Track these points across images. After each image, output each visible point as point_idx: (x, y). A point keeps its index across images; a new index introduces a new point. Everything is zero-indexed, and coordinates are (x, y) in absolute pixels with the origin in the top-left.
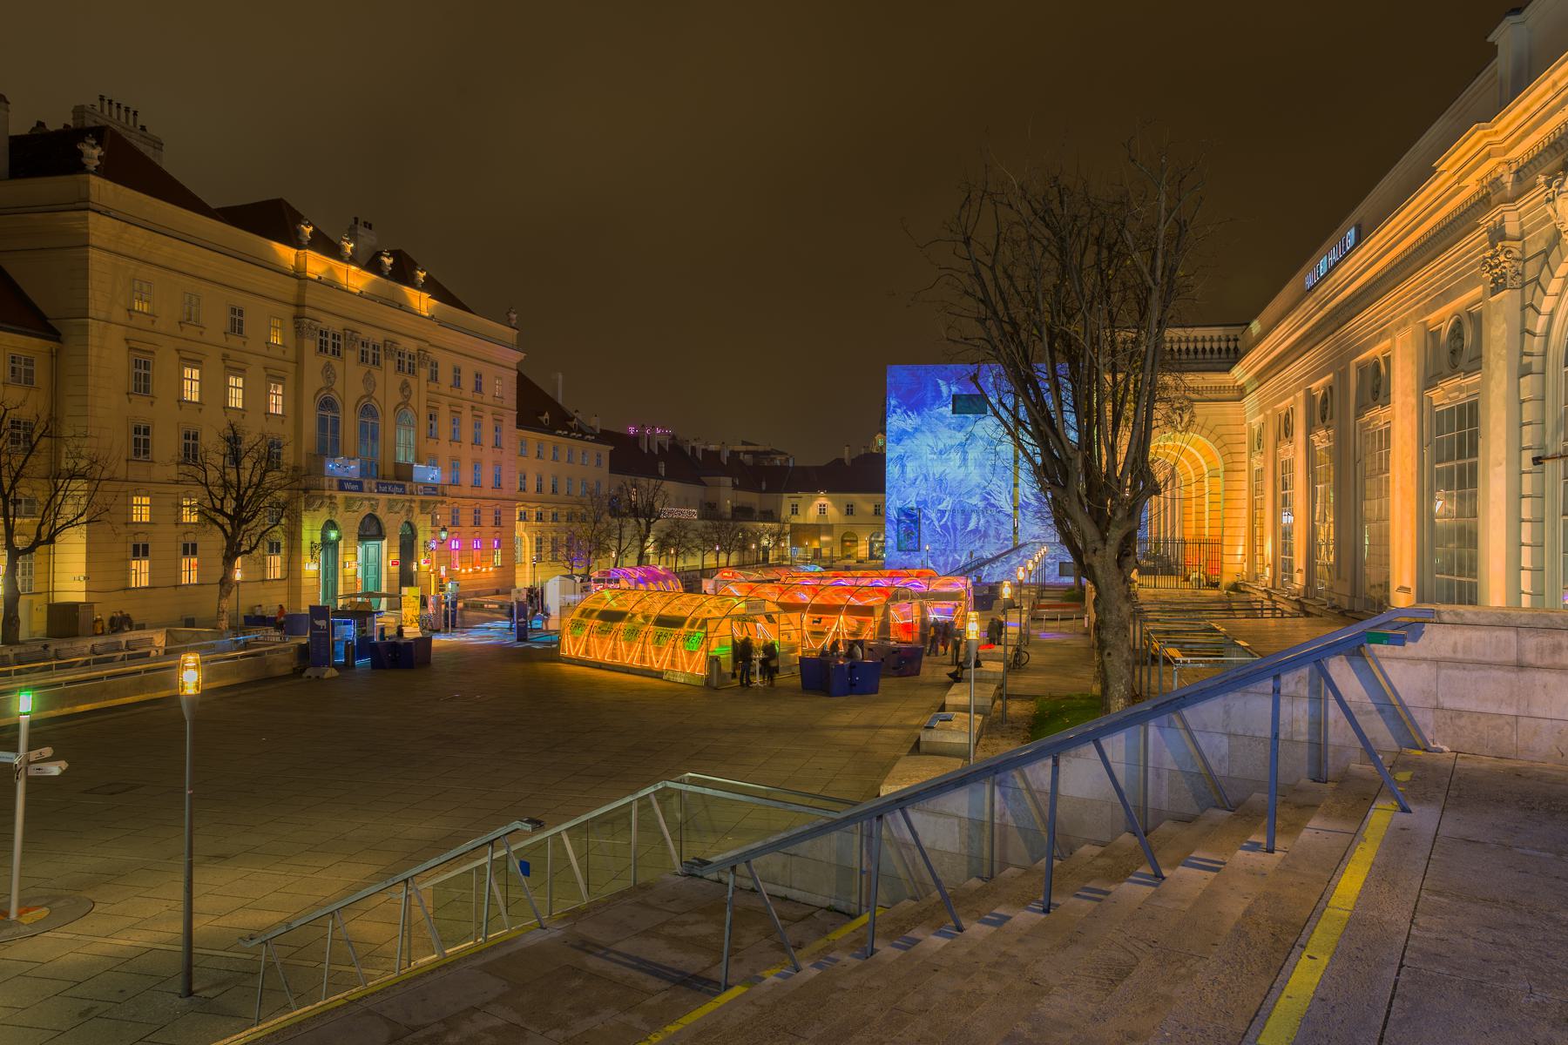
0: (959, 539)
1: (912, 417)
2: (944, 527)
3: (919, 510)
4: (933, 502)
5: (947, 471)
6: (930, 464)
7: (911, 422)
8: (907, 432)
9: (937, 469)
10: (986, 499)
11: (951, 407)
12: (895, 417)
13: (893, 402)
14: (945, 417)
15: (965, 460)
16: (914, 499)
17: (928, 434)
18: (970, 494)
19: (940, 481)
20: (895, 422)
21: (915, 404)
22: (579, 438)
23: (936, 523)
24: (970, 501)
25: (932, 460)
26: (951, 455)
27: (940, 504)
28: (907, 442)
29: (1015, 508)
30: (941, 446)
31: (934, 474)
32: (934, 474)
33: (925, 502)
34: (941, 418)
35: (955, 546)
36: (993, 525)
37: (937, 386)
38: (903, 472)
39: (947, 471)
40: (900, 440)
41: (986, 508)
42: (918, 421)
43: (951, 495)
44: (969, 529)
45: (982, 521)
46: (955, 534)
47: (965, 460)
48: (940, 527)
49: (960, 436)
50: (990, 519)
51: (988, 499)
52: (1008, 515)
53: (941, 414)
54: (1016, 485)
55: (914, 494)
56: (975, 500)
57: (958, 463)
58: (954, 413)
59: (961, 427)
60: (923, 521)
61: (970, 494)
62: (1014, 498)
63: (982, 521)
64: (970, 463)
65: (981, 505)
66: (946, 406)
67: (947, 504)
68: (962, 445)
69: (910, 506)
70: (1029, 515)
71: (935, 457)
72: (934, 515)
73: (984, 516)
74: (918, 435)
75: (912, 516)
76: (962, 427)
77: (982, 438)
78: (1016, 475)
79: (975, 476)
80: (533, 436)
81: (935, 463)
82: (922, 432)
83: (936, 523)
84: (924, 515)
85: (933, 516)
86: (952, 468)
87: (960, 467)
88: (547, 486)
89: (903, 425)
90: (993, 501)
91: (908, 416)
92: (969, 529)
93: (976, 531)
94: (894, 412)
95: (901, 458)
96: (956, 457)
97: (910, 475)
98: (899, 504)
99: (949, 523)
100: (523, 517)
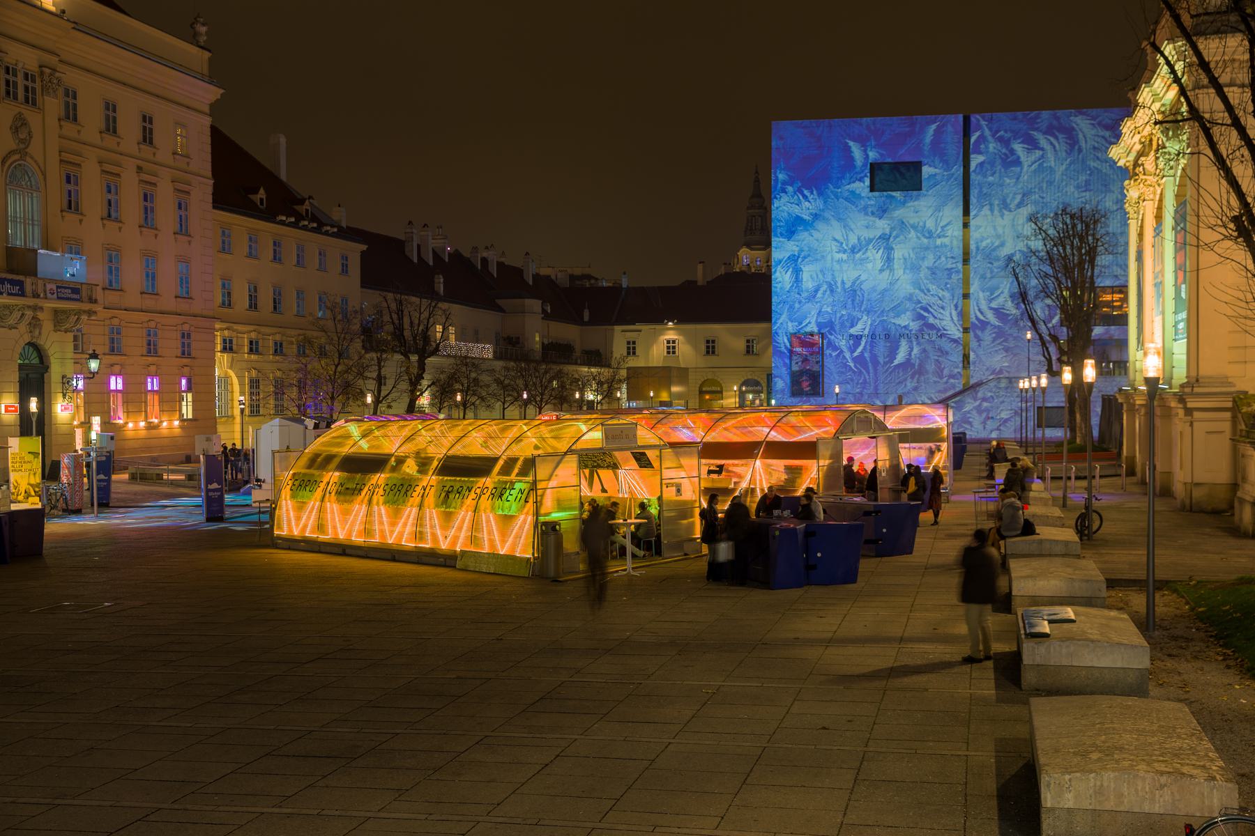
2: (859, 360)
3: (823, 336)
4: (842, 324)
5: (862, 278)
6: (837, 267)
9: (848, 275)
16: (813, 321)
17: (834, 223)
18: (897, 310)
19: (853, 293)
23: (847, 355)
25: (840, 261)
26: (869, 254)
27: (852, 326)
30: (853, 240)
31: (843, 282)
32: (843, 282)
33: (830, 324)
35: (876, 388)
38: (797, 280)
39: (862, 278)
43: (868, 312)
48: (855, 360)
49: (882, 225)
54: (966, 296)
55: (814, 312)
57: (879, 265)
60: (827, 352)
61: (897, 310)
62: (963, 315)
67: (862, 326)
68: (885, 238)
69: (808, 329)
71: (845, 257)
72: (843, 343)
75: (812, 345)
81: (845, 267)
83: (847, 355)
84: (830, 344)
85: (843, 344)
87: (881, 271)
96: (876, 257)
97: (808, 283)
98: (791, 327)
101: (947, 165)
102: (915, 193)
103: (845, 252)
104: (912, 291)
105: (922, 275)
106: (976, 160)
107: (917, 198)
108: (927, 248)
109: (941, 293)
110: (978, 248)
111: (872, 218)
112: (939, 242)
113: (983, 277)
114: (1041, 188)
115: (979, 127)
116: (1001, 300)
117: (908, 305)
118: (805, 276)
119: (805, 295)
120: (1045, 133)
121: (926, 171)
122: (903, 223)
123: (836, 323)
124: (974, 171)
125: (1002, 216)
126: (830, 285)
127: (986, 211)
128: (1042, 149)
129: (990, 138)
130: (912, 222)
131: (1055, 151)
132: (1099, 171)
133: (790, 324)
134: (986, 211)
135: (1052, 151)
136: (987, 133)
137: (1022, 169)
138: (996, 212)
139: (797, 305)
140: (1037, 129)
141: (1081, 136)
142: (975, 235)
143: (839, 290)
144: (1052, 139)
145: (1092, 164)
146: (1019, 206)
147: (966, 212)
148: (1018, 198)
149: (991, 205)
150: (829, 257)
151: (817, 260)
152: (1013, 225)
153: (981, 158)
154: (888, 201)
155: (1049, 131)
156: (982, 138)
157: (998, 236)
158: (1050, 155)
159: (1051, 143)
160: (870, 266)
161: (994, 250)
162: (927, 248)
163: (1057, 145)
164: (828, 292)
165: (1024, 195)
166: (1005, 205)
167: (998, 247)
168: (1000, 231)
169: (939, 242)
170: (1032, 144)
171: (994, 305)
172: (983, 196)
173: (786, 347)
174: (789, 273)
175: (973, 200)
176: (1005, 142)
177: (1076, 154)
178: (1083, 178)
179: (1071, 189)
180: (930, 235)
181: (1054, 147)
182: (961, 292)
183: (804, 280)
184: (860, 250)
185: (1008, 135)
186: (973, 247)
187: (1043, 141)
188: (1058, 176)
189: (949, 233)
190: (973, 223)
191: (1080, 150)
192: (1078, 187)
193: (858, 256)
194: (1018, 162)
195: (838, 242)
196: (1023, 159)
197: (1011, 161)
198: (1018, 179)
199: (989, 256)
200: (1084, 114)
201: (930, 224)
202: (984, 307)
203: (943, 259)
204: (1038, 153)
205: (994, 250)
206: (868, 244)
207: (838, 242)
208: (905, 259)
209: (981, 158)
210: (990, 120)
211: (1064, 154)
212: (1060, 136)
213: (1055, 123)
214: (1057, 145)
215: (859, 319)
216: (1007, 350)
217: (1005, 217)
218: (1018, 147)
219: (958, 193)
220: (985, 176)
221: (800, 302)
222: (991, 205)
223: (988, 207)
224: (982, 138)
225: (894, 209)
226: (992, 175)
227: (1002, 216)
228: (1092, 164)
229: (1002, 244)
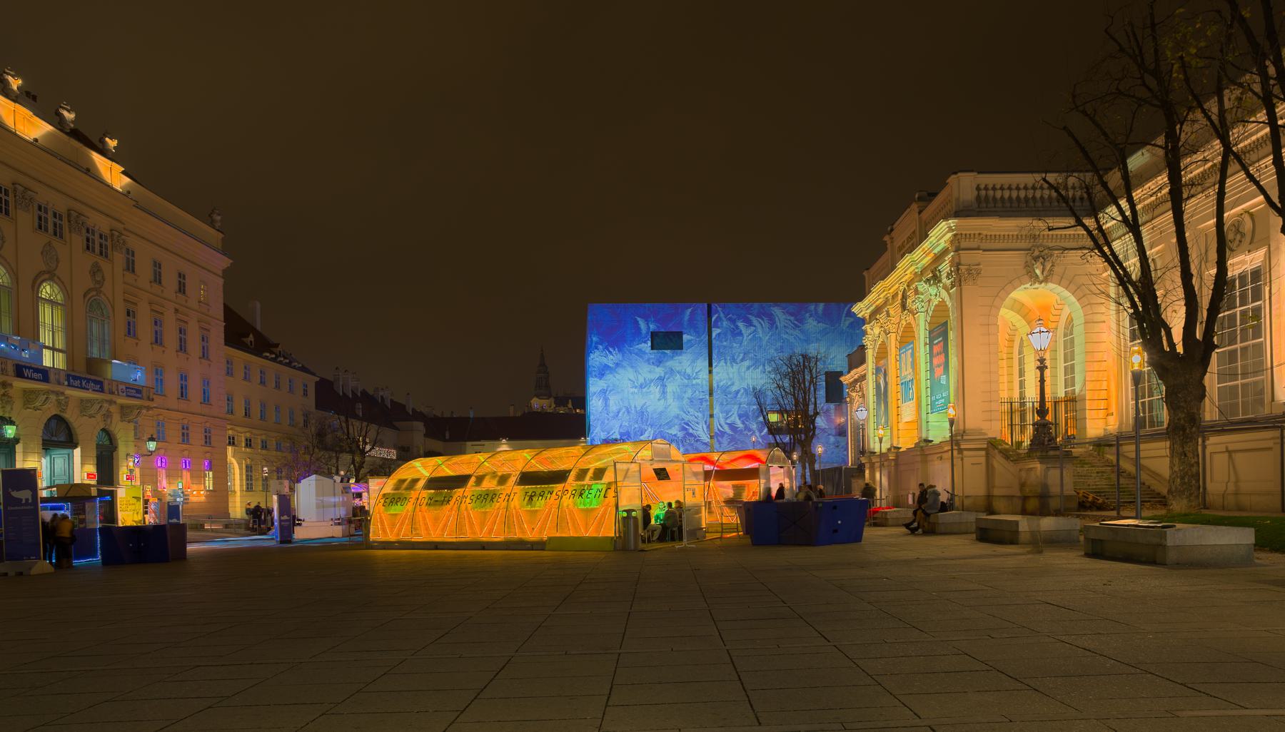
4: (635, 434)
5: (647, 404)
7: (611, 358)
8: (608, 366)
9: (638, 402)
11: (649, 344)
12: (597, 353)
13: (595, 339)
14: (645, 353)
15: (664, 393)
16: (617, 431)
17: (630, 370)
18: (670, 425)
19: (642, 413)
20: (596, 358)
21: (617, 339)
22: (286, 364)
24: (670, 431)
26: (651, 389)
27: (642, 435)
28: (610, 378)
29: (712, 437)
30: (641, 380)
31: (635, 407)
32: (635, 407)
34: (641, 353)
37: (636, 323)
38: (606, 405)
39: (647, 404)
40: (603, 375)
41: (684, 437)
42: (619, 356)
47: (664, 393)
49: (659, 371)
50: (689, 448)
51: (686, 429)
52: (705, 444)
53: (640, 350)
54: (711, 416)
55: (617, 426)
57: (658, 396)
58: (652, 349)
59: (659, 362)
61: (670, 425)
64: (669, 396)
65: (680, 434)
66: (645, 342)
68: (661, 379)
69: (614, 437)
70: (725, 441)
71: (636, 390)
73: (683, 446)
74: (620, 370)
76: (660, 362)
77: (678, 372)
78: (711, 407)
79: (674, 409)
80: (239, 356)
82: (624, 367)
86: (652, 401)
87: (659, 400)
88: (256, 411)
89: (604, 360)
90: (691, 431)
91: (609, 352)
94: (597, 348)
95: (604, 392)
96: (655, 390)
97: (613, 407)
100: (232, 442)
101: (698, 334)
102: (679, 351)
103: (636, 387)
105: (684, 402)
106: (715, 332)
107: (681, 354)
108: (687, 386)
109: (696, 414)
110: (718, 386)
111: (653, 366)
112: (694, 382)
113: (722, 404)
114: (754, 350)
115: (717, 312)
116: (732, 418)
117: (676, 421)
118: (611, 402)
119: (611, 415)
120: (756, 317)
121: (685, 337)
122: (672, 369)
123: (632, 432)
124: (715, 338)
125: (732, 366)
127: (722, 363)
128: (755, 326)
129: (724, 319)
130: (677, 369)
131: (762, 327)
132: (788, 340)
133: (602, 433)
134: (722, 363)
135: (761, 327)
136: (722, 315)
137: (743, 338)
138: (728, 364)
139: (606, 421)
140: (751, 314)
141: (777, 319)
142: (716, 377)
143: (633, 412)
144: (760, 321)
145: (785, 336)
146: (742, 360)
147: (710, 365)
148: (742, 355)
149: (725, 359)
150: (626, 391)
151: (618, 392)
152: (739, 372)
153: (718, 331)
154: (662, 356)
155: (759, 316)
156: (719, 319)
157: (730, 379)
158: (760, 331)
159: (760, 323)
160: (652, 396)
161: (728, 387)
162: (687, 386)
163: (762, 323)
165: (745, 354)
166: (734, 360)
167: (730, 385)
168: (731, 376)
169: (694, 382)
170: (749, 323)
171: (728, 421)
172: (720, 354)
174: (601, 401)
175: (714, 356)
176: (733, 321)
177: (774, 329)
178: (779, 344)
179: (772, 351)
180: (689, 378)
181: (762, 325)
182: (709, 413)
183: (611, 405)
184: (645, 387)
185: (735, 317)
186: (715, 385)
187: (755, 321)
188: (764, 343)
189: (700, 376)
190: (715, 370)
191: (777, 328)
192: (776, 350)
193: (644, 390)
194: (740, 334)
195: (632, 381)
196: (743, 332)
197: (736, 333)
198: (741, 344)
199: (725, 390)
200: (778, 306)
201: (689, 371)
202: (722, 422)
203: (697, 392)
204: (753, 328)
205: (728, 387)
206: (651, 383)
207: (632, 381)
208: (674, 392)
209: (718, 331)
210: (723, 307)
211: (768, 329)
212: (765, 319)
213: (762, 310)
214: (762, 323)
215: (646, 430)
217: (734, 367)
218: (741, 325)
219: (706, 351)
220: (721, 342)
221: (608, 419)
222: (725, 359)
223: (723, 361)
224: (717, 320)
225: (667, 361)
226: (726, 341)
227: (732, 366)
228: (785, 336)
229: (733, 384)
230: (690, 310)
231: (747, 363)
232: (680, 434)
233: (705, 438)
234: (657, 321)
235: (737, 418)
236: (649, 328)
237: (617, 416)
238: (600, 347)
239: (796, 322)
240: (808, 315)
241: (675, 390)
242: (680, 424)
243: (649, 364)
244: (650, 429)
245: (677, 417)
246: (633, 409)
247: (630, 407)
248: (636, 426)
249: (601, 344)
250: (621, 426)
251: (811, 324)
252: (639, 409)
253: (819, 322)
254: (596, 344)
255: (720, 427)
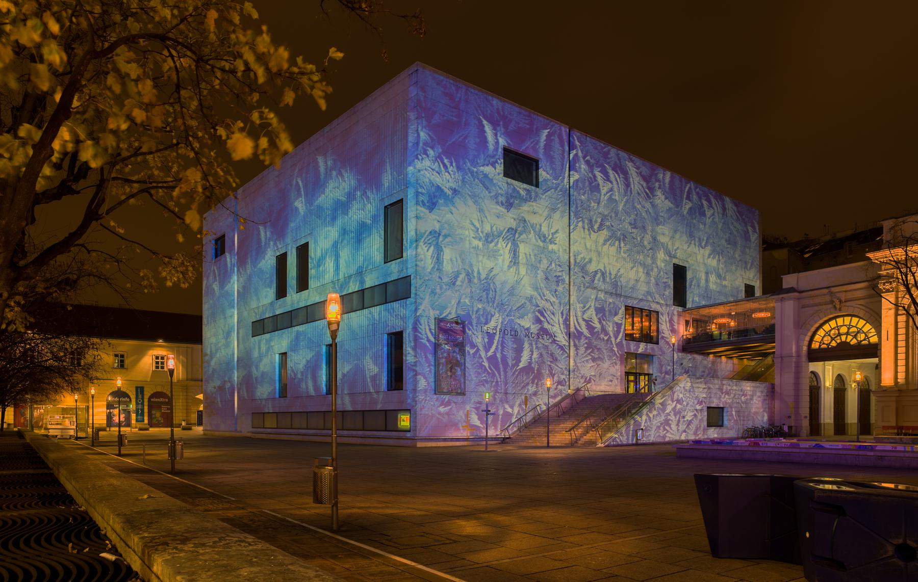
0: (510, 380)
1: (450, 169)
10: (538, 321)
19: (487, 287)
23: (483, 353)
30: (487, 228)
36: (548, 362)
38: (438, 260)
44: (521, 365)
45: (535, 355)
46: (505, 372)
49: (509, 220)
50: (544, 353)
55: (454, 302)
56: (527, 322)
63: (535, 355)
66: (493, 165)
68: (512, 231)
89: (437, 180)
90: (546, 325)
92: (521, 365)
93: (528, 369)
96: (504, 248)
97: (447, 267)
99: (499, 355)
104: (533, 293)
112: (551, 247)
119: (445, 280)
126: (468, 275)
143: (476, 280)
164: (467, 281)
173: (428, 340)
215: (492, 316)
216: (594, 360)
230: (546, 132)
231: (605, 233)
232: (534, 329)
233: (562, 338)
234: (507, 134)
235: (594, 313)
236: (497, 143)
237: (454, 284)
238: (431, 152)
239: (647, 191)
240: (657, 184)
241: (528, 253)
242: (534, 312)
243: (497, 203)
244: (497, 315)
245: (530, 299)
246: (475, 274)
247: (473, 271)
248: (480, 306)
249: (432, 148)
250: (459, 302)
251: (661, 200)
252: (483, 276)
253: (666, 198)
254: (424, 144)
255: (576, 324)
